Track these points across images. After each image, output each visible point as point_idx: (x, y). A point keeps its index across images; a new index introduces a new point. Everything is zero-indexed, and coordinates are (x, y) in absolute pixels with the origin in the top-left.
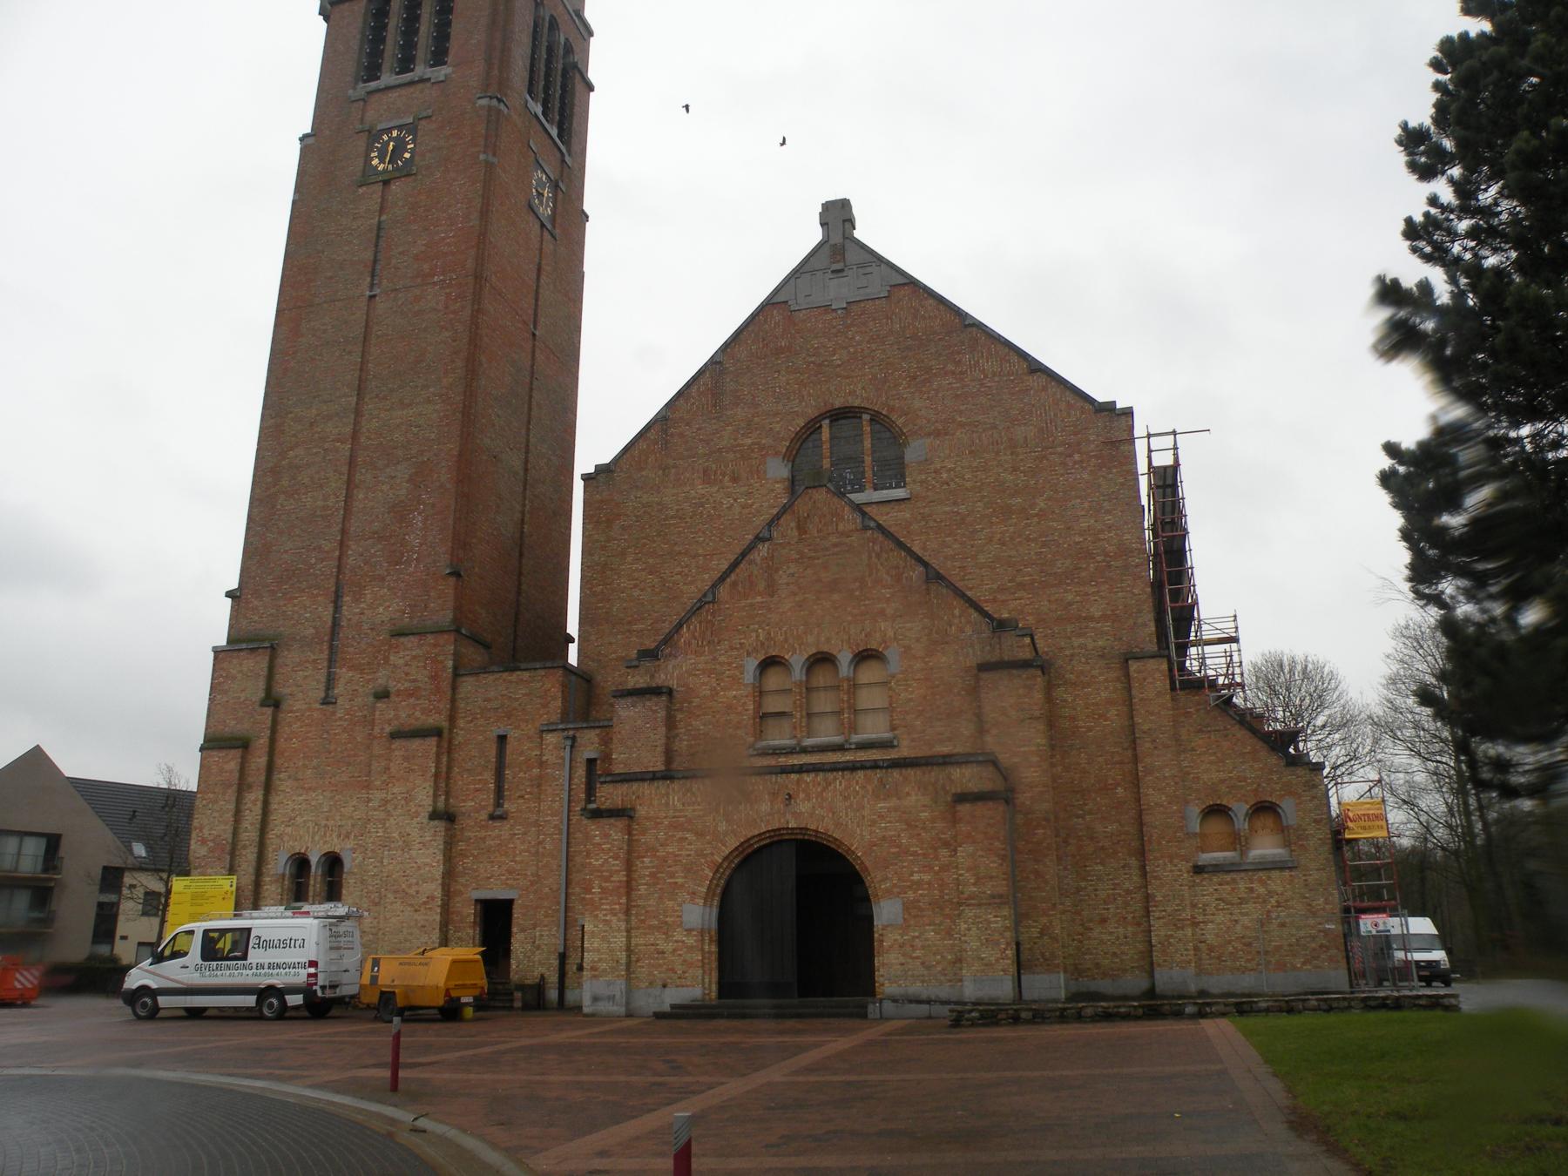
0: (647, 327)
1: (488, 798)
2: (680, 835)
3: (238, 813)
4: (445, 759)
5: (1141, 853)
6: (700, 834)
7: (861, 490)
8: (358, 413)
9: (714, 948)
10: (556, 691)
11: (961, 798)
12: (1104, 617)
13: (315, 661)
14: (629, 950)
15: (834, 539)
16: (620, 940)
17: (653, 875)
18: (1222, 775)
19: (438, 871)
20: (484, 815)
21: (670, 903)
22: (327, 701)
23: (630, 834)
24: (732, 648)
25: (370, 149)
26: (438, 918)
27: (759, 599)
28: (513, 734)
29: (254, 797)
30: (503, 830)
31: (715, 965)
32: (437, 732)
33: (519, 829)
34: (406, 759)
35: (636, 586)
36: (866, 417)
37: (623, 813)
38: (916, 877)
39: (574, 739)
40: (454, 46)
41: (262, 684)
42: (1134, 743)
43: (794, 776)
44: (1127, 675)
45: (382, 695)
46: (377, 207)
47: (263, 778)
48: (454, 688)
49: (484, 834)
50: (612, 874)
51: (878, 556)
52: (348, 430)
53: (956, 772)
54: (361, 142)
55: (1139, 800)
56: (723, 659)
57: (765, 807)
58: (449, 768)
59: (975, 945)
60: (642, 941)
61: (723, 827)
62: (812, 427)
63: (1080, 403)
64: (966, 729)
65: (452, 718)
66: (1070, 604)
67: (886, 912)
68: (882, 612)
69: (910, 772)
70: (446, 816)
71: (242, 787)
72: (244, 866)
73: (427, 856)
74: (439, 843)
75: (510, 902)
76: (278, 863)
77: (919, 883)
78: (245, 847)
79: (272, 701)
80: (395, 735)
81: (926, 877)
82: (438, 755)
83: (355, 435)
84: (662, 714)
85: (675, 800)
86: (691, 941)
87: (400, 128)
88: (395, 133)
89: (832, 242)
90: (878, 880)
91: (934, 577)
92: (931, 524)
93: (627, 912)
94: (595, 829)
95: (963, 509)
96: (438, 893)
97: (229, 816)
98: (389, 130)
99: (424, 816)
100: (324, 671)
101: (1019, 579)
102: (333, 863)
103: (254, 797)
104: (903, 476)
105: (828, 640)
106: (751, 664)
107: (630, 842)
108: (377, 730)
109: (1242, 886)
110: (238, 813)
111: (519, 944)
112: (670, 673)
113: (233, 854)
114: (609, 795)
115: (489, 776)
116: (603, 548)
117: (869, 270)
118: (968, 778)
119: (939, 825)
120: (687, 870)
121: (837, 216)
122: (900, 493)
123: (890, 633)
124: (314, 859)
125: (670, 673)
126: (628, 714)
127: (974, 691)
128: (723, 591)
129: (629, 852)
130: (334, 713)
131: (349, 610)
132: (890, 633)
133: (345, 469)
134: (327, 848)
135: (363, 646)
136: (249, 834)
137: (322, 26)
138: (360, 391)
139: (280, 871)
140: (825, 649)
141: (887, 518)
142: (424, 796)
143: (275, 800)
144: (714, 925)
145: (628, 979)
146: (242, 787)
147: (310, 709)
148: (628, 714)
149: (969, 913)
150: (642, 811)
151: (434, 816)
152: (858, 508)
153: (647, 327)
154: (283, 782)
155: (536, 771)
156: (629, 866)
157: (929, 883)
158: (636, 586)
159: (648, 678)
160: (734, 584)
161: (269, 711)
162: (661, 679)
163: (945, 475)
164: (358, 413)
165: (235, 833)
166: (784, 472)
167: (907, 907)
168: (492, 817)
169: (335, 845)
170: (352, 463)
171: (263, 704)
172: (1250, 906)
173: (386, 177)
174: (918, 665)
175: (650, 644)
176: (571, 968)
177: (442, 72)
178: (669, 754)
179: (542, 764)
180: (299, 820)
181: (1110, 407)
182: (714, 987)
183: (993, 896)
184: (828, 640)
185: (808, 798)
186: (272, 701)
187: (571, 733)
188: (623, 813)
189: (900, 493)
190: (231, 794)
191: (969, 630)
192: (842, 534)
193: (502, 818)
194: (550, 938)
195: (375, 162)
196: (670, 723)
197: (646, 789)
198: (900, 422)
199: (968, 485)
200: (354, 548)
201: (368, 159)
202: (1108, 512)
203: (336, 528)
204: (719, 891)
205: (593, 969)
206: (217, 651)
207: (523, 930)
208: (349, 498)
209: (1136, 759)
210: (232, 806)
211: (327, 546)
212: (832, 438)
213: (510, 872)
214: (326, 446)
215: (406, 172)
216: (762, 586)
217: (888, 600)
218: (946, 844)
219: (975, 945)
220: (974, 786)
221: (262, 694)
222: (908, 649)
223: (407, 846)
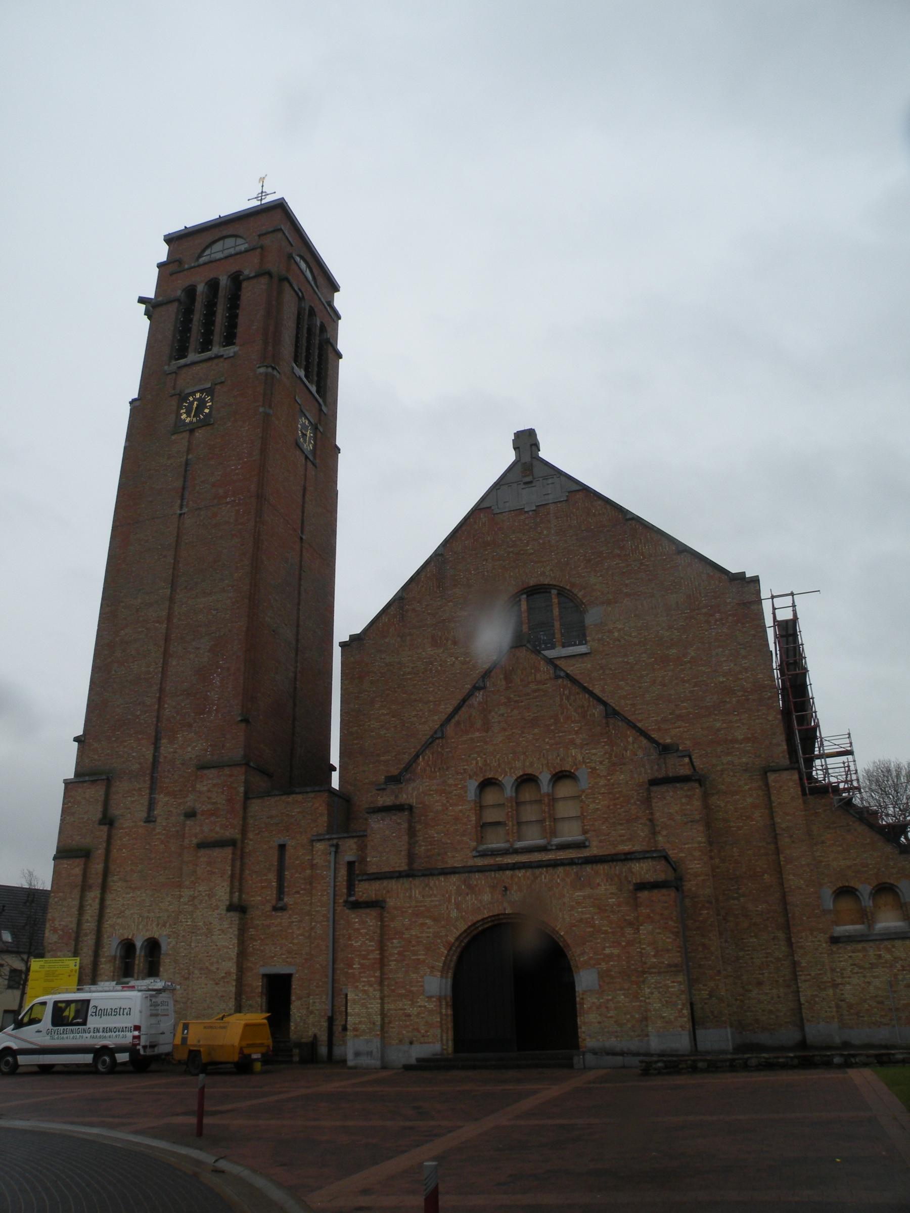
0: (385, 531)
1: (271, 894)
2: (421, 921)
3: (81, 909)
4: (238, 864)
5: (787, 927)
6: (435, 919)
7: (553, 647)
8: (171, 599)
9: (450, 1012)
10: (323, 809)
11: (641, 886)
12: (747, 740)
13: (140, 789)
14: (383, 1014)
15: (533, 686)
16: (375, 1006)
17: (400, 953)
19: (233, 953)
20: (268, 907)
21: (414, 976)
22: (150, 819)
23: (382, 920)
24: (458, 773)
25: (180, 407)
26: (233, 989)
27: (477, 734)
28: (291, 843)
29: (93, 895)
31: (450, 1025)
32: (232, 843)
33: (296, 918)
36: (554, 592)
37: (376, 904)
38: (607, 951)
39: (337, 846)
40: (240, 330)
41: (100, 808)
42: (775, 838)
43: (508, 873)
44: (767, 785)
45: (191, 814)
47: (100, 881)
48: (245, 808)
51: (568, 698)
53: (636, 867)
54: (174, 402)
55: (782, 884)
56: (451, 782)
57: (486, 898)
58: (242, 871)
59: (657, 1006)
60: (392, 1006)
61: (454, 914)
65: (244, 831)
66: (719, 730)
67: (585, 980)
68: (572, 742)
69: (600, 868)
70: (239, 908)
71: (85, 887)
72: (85, 950)
73: (225, 941)
74: (234, 930)
75: (289, 976)
76: (111, 947)
77: (610, 957)
78: (86, 935)
79: (108, 821)
80: (202, 845)
81: (616, 951)
82: (233, 860)
83: (169, 619)
84: (405, 825)
85: (416, 893)
86: (431, 1006)
88: (198, 395)
89: (523, 461)
90: (578, 954)
91: (612, 713)
92: (607, 672)
93: (381, 983)
94: (354, 918)
95: (631, 659)
96: (234, 970)
97: (75, 911)
98: (193, 394)
100: (147, 797)
101: (678, 712)
102: (153, 946)
103: (93, 895)
104: (584, 635)
105: (532, 764)
106: (473, 785)
107: (382, 927)
108: (187, 842)
110: (81, 909)
113: (77, 940)
114: (366, 890)
115: (272, 876)
118: (644, 870)
121: (526, 442)
122: (582, 649)
123: (580, 758)
124: (138, 944)
125: (409, 794)
126: (379, 826)
127: (647, 802)
128: (450, 730)
129: (382, 935)
130: (154, 829)
131: (166, 749)
132: (580, 758)
134: (148, 935)
136: (90, 924)
137: (146, 323)
138: (173, 585)
139: (113, 953)
140: (529, 771)
141: (573, 669)
142: (222, 893)
143: (109, 897)
144: (449, 993)
145: (383, 1038)
146: (85, 887)
148: (379, 826)
149: (652, 979)
150: (391, 902)
151: (231, 908)
152: (551, 661)
153: (385, 531)
154: (116, 883)
155: (308, 872)
156: (382, 947)
157: (619, 956)
159: (393, 798)
160: (458, 723)
161: (105, 828)
162: (403, 798)
163: (616, 634)
164: (171, 599)
165: (79, 924)
167: (602, 975)
168: (275, 909)
169: (155, 932)
170: (167, 639)
171: (102, 822)
173: (191, 427)
175: (394, 771)
176: (338, 1029)
177: (231, 350)
178: (411, 857)
179: (313, 866)
180: (127, 913)
181: (741, 576)
182: (450, 1044)
183: (669, 966)
184: (532, 764)
186: (108, 821)
187: (335, 842)
188: (376, 904)
189: (582, 649)
190: (76, 893)
191: (640, 754)
192: (539, 682)
193: (283, 909)
194: (320, 1004)
195: (184, 417)
196: (412, 832)
197: (393, 884)
198: (580, 594)
199: (635, 640)
201: (179, 415)
202: (744, 657)
204: (452, 965)
205: (355, 1030)
206: (67, 783)
207: (299, 998)
208: (165, 664)
209: (778, 852)
210: (76, 903)
213: (289, 952)
215: (206, 423)
216: (479, 724)
217: (577, 733)
218: (630, 924)
219: (657, 1006)
220: (650, 877)
221: (99, 816)
222: (594, 769)
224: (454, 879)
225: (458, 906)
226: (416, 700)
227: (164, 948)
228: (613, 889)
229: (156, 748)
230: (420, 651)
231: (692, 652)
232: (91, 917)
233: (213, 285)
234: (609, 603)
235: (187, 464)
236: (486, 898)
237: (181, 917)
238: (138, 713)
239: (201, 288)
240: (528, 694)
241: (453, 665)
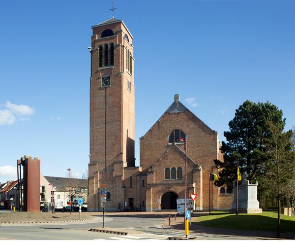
1: (129, 185)
20: (129, 187)
30: (131, 189)
73: (122, 192)
74: (123, 191)
99: (121, 187)
111: (135, 203)
121: (176, 97)
151: (123, 187)
194: (139, 202)
223: (119, 191)
233: (106, 46)
239: (103, 47)
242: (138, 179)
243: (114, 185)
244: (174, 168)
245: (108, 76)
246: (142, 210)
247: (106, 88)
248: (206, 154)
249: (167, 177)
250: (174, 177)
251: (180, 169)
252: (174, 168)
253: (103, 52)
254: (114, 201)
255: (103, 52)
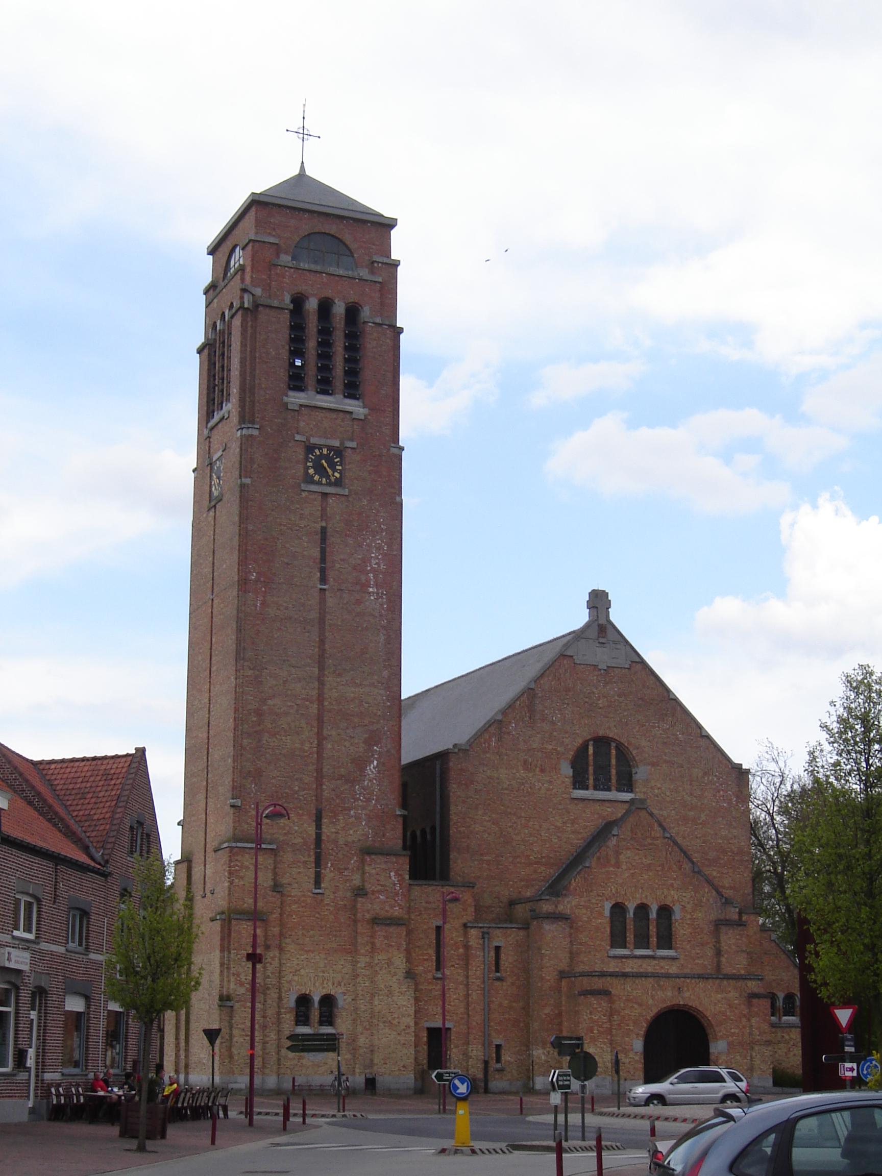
2: (630, 1005)
6: (641, 1005)
8: (321, 683)
12: (731, 888)
13: (305, 862)
15: (649, 841)
17: (619, 1025)
18: (774, 977)
19: (412, 1011)
20: (430, 976)
24: (599, 896)
25: (307, 459)
26: (413, 1039)
27: (611, 869)
34: (386, 937)
35: (485, 831)
36: (613, 745)
38: (733, 1031)
43: (682, 979)
45: (360, 892)
46: (319, 513)
49: (430, 987)
50: (603, 1023)
52: (315, 693)
53: (749, 983)
54: (300, 453)
56: (594, 901)
57: (669, 994)
59: (758, 1062)
61: (650, 1002)
62: (585, 746)
63: (725, 761)
64: (710, 952)
68: (672, 885)
69: (732, 982)
73: (404, 1001)
76: (290, 1001)
78: (268, 988)
81: (737, 1031)
87: (330, 448)
89: (600, 622)
100: (313, 870)
102: (328, 1001)
105: (646, 897)
106: (608, 906)
109: (779, 1034)
112: (567, 905)
115: (432, 952)
116: (464, 802)
117: (618, 646)
118: (753, 986)
119: (743, 1007)
120: (635, 1022)
121: (598, 601)
123: (676, 897)
125: (567, 905)
130: (322, 900)
132: (676, 897)
133: (315, 723)
134: (325, 992)
135: (340, 856)
140: (645, 901)
142: (399, 961)
147: (304, 896)
158: (485, 831)
162: (561, 908)
166: (570, 772)
167: (729, 1044)
170: (320, 719)
172: (781, 1045)
174: (689, 916)
177: (355, 407)
180: (303, 972)
184: (646, 897)
185: (688, 990)
191: (711, 900)
194: (476, 1051)
197: (615, 981)
198: (634, 752)
199: (668, 799)
200: (327, 786)
202: (734, 828)
203: (312, 768)
207: (457, 1047)
211: (307, 779)
212: (594, 753)
214: (299, 702)
216: (613, 861)
218: (745, 1016)
219: (758, 1062)
220: (756, 990)
221: (272, 883)
222: (684, 907)
223: (390, 994)
224: (651, 980)
225: (653, 997)
226: (510, 813)
227: (340, 1003)
228: (737, 995)
229: (319, 826)
230: (514, 771)
231: (703, 817)
232: (272, 973)
233: (325, 307)
234: (653, 765)
235: (324, 530)
236: (669, 994)
237: (360, 979)
238: (297, 788)
240: (645, 846)
241: (540, 789)
242: (473, 942)
243: (363, 961)
244: (642, 909)
245: (337, 443)
246: (494, 1084)
247: (325, 495)
248: (712, 855)
249: (618, 939)
250: (642, 941)
251: (665, 911)
252: (642, 909)
253: (312, 325)
254: (362, 1040)
255: (312, 325)
